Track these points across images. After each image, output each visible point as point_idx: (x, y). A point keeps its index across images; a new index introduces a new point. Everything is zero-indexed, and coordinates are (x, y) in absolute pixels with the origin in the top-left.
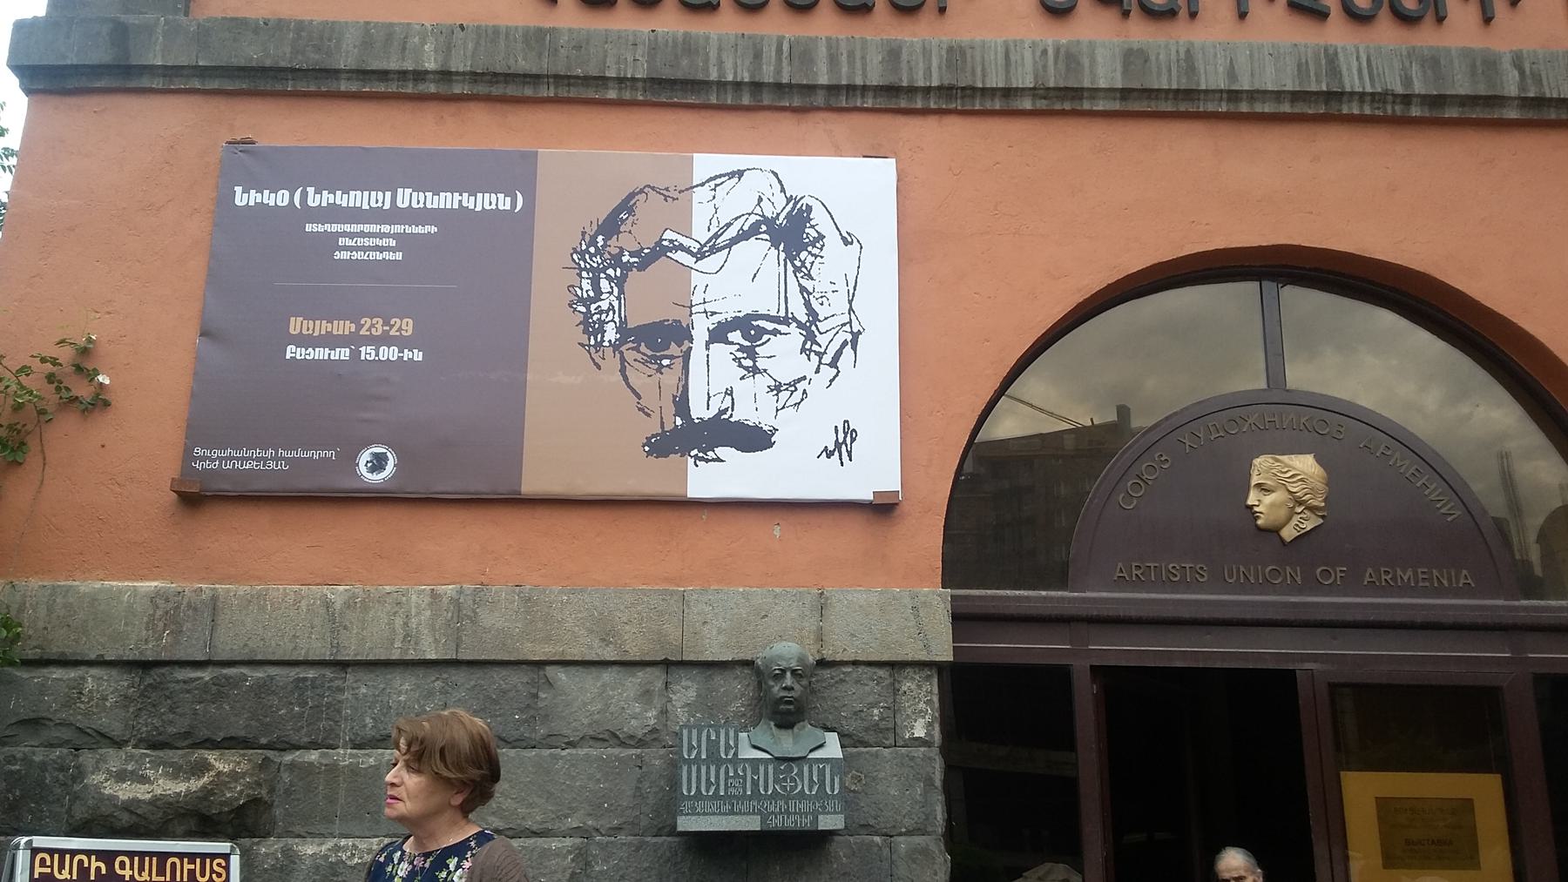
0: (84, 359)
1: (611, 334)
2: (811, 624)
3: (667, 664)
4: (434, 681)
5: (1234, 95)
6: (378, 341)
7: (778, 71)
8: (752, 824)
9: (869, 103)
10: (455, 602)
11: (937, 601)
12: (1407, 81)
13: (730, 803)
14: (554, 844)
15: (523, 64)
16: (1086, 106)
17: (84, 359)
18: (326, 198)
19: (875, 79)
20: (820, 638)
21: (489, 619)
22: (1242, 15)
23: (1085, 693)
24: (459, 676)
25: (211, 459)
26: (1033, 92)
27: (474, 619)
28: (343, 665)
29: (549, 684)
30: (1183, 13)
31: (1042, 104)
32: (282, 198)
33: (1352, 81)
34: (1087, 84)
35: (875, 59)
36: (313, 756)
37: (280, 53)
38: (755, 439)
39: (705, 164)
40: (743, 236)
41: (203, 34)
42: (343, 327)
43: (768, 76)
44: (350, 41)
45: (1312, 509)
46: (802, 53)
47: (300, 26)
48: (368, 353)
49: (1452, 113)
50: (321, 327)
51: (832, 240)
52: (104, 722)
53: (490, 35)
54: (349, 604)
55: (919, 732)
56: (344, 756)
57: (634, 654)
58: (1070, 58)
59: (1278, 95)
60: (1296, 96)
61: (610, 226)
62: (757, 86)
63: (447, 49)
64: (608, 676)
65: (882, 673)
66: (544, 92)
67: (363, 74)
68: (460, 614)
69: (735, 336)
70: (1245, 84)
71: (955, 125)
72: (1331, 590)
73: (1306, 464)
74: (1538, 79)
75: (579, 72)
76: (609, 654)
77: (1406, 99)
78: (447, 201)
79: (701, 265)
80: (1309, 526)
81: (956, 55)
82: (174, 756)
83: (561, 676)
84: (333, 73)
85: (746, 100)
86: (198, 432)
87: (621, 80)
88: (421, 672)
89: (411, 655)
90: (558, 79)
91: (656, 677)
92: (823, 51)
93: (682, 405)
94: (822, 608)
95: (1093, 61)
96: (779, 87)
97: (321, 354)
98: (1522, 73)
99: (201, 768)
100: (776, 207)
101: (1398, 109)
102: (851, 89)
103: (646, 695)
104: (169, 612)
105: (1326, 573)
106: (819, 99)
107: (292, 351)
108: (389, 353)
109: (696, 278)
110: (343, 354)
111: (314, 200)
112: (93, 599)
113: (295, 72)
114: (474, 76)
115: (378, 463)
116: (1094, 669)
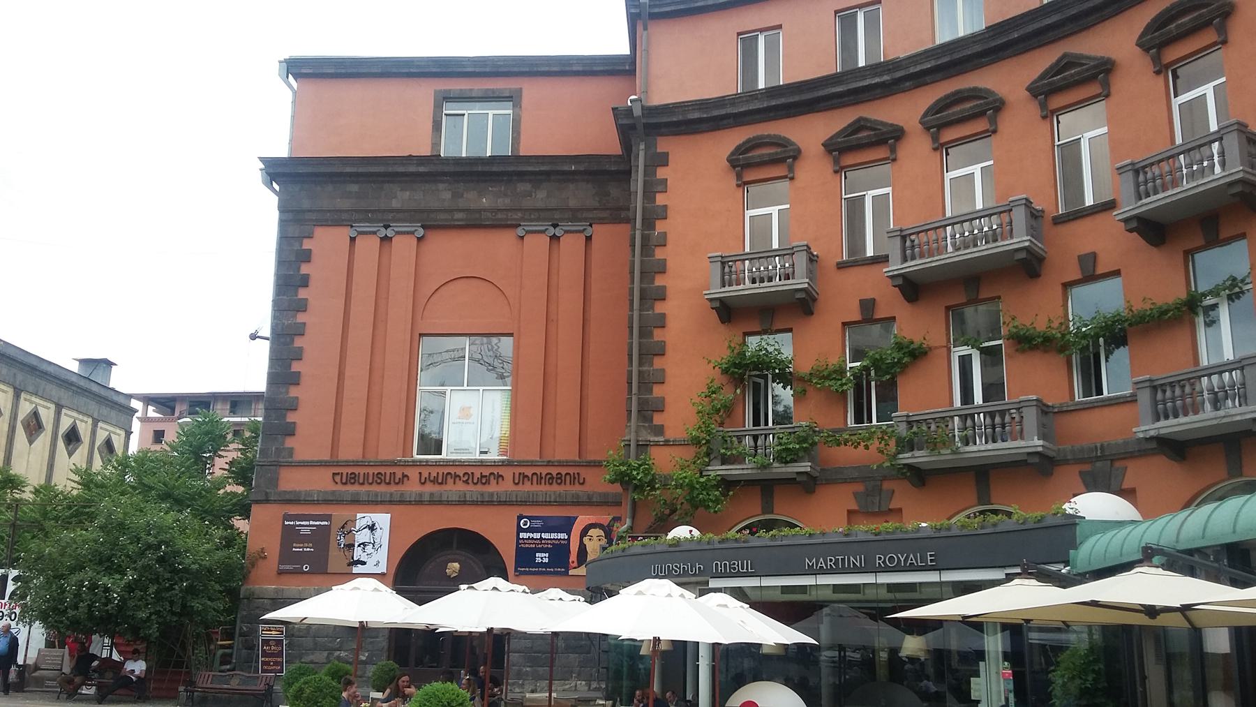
0: (263, 550)
1: (342, 546)
5: (449, 501)
6: (307, 548)
15: (331, 499)
17: (263, 550)
18: (299, 523)
22: (454, 483)
25: (282, 567)
26: (415, 501)
30: (444, 482)
32: (292, 523)
33: (468, 499)
35: (388, 495)
37: (292, 497)
38: (364, 563)
39: (359, 516)
40: (364, 528)
42: (302, 545)
43: (370, 499)
44: (303, 493)
46: (376, 495)
47: (295, 491)
48: (305, 550)
50: (298, 545)
51: (379, 528)
52: (268, 607)
53: (326, 492)
54: (302, 589)
58: (421, 495)
59: (455, 501)
60: (458, 501)
61: (343, 527)
62: (368, 501)
66: (334, 502)
69: (362, 546)
70: (450, 499)
73: (456, 565)
77: (477, 501)
78: (318, 523)
79: (359, 533)
81: (402, 494)
86: (281, 562)
90: (337, 501)
93: (353, 558)
97: (298, 550)
100: (370, 523)
102: (384, 501)
104: (276, 591)
107: (294, 549)
108: (308, 549)
109: (356, 536)
110: (301, 550)
111: (297, 523)
112: (266, 589)
113: (295, 500)
115: (306, 568)
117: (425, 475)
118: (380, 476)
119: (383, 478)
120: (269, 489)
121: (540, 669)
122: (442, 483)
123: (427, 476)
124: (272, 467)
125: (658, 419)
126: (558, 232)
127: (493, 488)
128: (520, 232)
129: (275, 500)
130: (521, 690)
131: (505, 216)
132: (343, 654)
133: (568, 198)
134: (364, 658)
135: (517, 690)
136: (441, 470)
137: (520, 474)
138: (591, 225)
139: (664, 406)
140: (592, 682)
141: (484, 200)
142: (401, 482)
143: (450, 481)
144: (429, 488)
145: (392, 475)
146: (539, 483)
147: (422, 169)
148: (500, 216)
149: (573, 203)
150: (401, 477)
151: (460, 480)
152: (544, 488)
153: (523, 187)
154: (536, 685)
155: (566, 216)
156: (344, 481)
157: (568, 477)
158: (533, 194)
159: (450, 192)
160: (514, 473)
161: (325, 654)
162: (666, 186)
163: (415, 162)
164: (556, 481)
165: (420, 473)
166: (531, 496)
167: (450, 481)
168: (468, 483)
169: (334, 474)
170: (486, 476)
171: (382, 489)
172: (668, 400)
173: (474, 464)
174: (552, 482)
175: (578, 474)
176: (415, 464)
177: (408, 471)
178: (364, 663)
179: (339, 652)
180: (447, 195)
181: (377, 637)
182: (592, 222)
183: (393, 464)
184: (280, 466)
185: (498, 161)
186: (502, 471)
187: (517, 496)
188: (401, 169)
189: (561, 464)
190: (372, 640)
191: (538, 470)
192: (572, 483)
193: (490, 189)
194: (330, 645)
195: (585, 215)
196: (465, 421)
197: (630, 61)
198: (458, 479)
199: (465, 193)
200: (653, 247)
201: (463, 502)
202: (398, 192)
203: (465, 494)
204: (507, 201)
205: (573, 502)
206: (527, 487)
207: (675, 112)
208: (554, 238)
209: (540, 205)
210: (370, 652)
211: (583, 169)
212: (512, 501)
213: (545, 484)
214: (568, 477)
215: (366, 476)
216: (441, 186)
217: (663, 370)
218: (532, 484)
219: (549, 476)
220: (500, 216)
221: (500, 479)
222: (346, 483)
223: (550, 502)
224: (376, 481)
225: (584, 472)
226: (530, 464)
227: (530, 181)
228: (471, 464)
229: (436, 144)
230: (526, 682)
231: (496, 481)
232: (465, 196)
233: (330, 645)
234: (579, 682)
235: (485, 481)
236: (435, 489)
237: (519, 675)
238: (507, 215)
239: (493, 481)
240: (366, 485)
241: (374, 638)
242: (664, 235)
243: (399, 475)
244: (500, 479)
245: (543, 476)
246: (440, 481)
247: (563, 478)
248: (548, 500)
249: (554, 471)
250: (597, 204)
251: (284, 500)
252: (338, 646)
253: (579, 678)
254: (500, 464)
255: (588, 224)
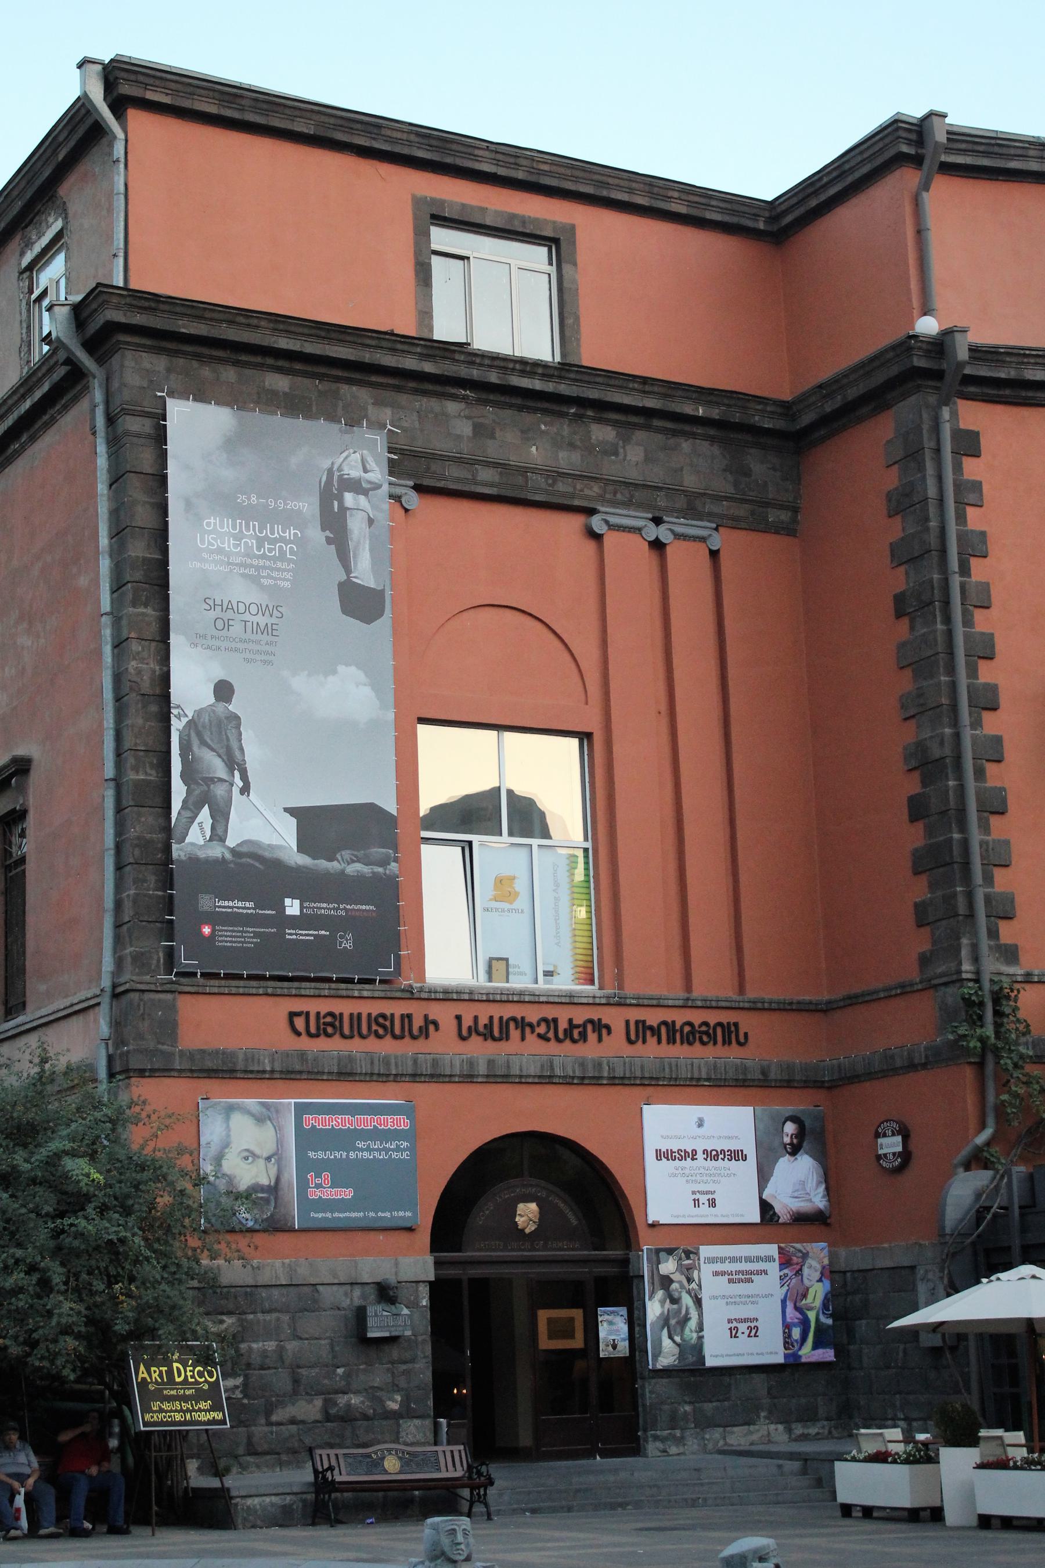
2: (394, 1270)
3: (352, 1284)
4: (284, 1290)
5: (521, 1076)
7: (379, 1070)
8: (387, 1334)
9: (407, 1079)
10: (289, 1265)
11: (430, 1259)
12: (574, 1072)
13: (380, 1328)
14: (323, 1342)
15: (298, 1067)
16: (475, 1080)
19: (410, 1072)
20: (396, 1274)
21: (300, 1271)
23: (465, 1285)
24: (291, 1289)
26: (459, 1076)
27: (295, 1271)
28: (256, 1286)
29: (318, 1291)
31: (461, 1080)
34: (476, 1073)
35: (410, 1063)
36: (251, 1316)
41: (191, 1056)
44: (241, 1057)
45: (534, 1222)
46: (386, 1061)
49: (586, 1081)
55: (424, 1303)
56: (260, 1316)
57: (343, 1281)
58: (471, 1063)
59: (534, 1077)
60: (540, 1077)
62: (372, 1074)
63: (272, 1061)
64: (335, 1288)
65: (414, 1284)
66: (305, 1076)
67: (246, 1071)
68: (291, 1270)
70: (524, 1073)
71: (434, 1087)
72: (538, 1250)
73: (533, 1206)
74: (614, 1071)
75: (316, 1070)
76: (336, 1281)
77: (573, 1078)
80: (533, 1229)
82: (213, 1317)
83: (320, 1288)
84: (235, 1071)
85: (368, 1079)
87: (329, 1073)
88: (280, 1288)
89: (278, 1283)
91: (348, 1287)
92: (393, 1061)
94: (397, 1264)
95: (478, 1064)
96: (379, 1075)
98: (609, 1067)
99: (222, 1322)
101: (571, 1080)
103: (346, 1294)
105: (537, 1245)
106: (391, 1078)
114: (281, 1072)
116: (470, 1279)
117: (468, 1022)
118: (381, 1020)
119: (388, 1023)
120: (163, 1044)
121: (706, 1405)
122: (500, 1039)
123: (471, 1023)
124: (162, 996)
125: (1007, 932)
126: (663, 533)
127: (591, 1050)
128: (597, 523)
129: (180, 1071)
130: (681, 1450)
131: (571, 490)
132: (355, 1400)
133: (682, 469)
134: (393, 1406)
135: (673, 1450)
136: (499, 1012)
137: (637, 1022)
138: (716, 529)
139: (1014, 908)
140: (794, 1426)
141: (534, 449)
142: (424, 1032)
143: (515, 1034)
144: (479, 1050)
145: (406, 1020)
146: (671, 1040)
147: (428, 367)
148: (561, 487)
149: (690, 481)
150: (422, 1024)
151: (533, 1032)
152: (679, 1052)
153: (602, 433)
154: (703, 1438)
155: (677, 506)
156: (313, 1030)
157: (719, 1031)
158: (621, 451)
159: (470, 423)
160: (627, 1022)
161: (318, 1402)
162: (981, 495)
163: (419, 350)
164: (701, 1039)
165: (458, 1018)
166: (667, 1070)
167: (515, 1034)
168: (548, 1040)
169: (292, 1015)
170: (578, 1026)
171: (386, 1047)
172: (1019, 900)
173: (557, 1000)
174: (694, 1038)
175: (736, 1025)
176: (450, 996)
177: (436, 1011)
178: (396, 1416)
179: (346, 1397)
180: (465, 429)
181: (414, 1362)
182: (719, 523)
183: (408, 995)
184: (180, 993)
185: (572, 376)
186: (608, 1016)
187: (642, 1067)
188: (388, 360)
189: (707, 1006)
190: (404, 1367)
191: (668, 1016)
192: (727, 1042)
193: (543, 427)
194: (326, 1381)
195: (710, 507)
196: (505, 906)
197: (767, 214)
198: (528, 1030)
199: (497, 430)
200: (971, 608)
201: (547, 1079)
202: (370, 408)
203: (552, 1063)
204: (576, 457)
205: (736, 1080)
206: (651, 1051)
207: (1004, 362)
208: (657, 545)
209: (634, 475)
210: (403, 1393)
211: (717, 417)
212: (635, 1078)
213: (682, 1043)
214: (719, 1031)
215: (356, 1019)
216: (452, 407)
217: (1007, 843)
218: (659, 1042)
219: (687, 1029)
220: (561, 487)
221: (604, 1031)
222: (317, 1036)
223: (699, 1079)
224: (376, 1032)
225: (747, 1022)
226: (655, 1002)
227: (615, 424)
228: (551, 999)
229: (425, 314)
230: (688, 1433)
231: (596, 1035)
232: (497, 435)
233: (326, 1381)
234: (772, 1427)
235: (576, 1033)
236: (490, 1049)
237: (674, 1421)
238: (575, 488)
239: (592, 1037)
240: (357, 1040)
241: (405, 1362)
242: (985, 588)
243: (418, 1022)
244: (604, 1031)
245: (678, 1027)
246: (496, 1033)
247: (711, 1031)
248: (696, 1076)
249: (697, 1017)
250: (730, 489)
251: (201, 1071)
252: (343, 1383)
253: (773, 1418)
254: (603, 1001)
255: (714, 525)
